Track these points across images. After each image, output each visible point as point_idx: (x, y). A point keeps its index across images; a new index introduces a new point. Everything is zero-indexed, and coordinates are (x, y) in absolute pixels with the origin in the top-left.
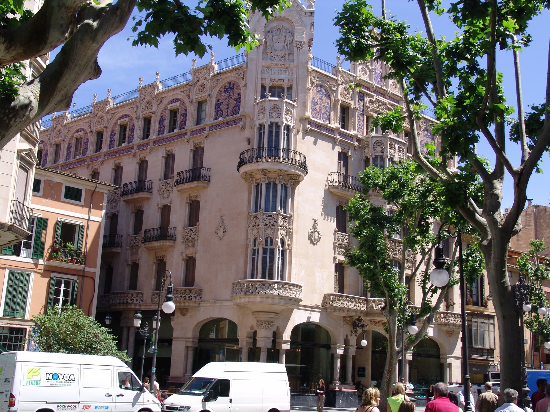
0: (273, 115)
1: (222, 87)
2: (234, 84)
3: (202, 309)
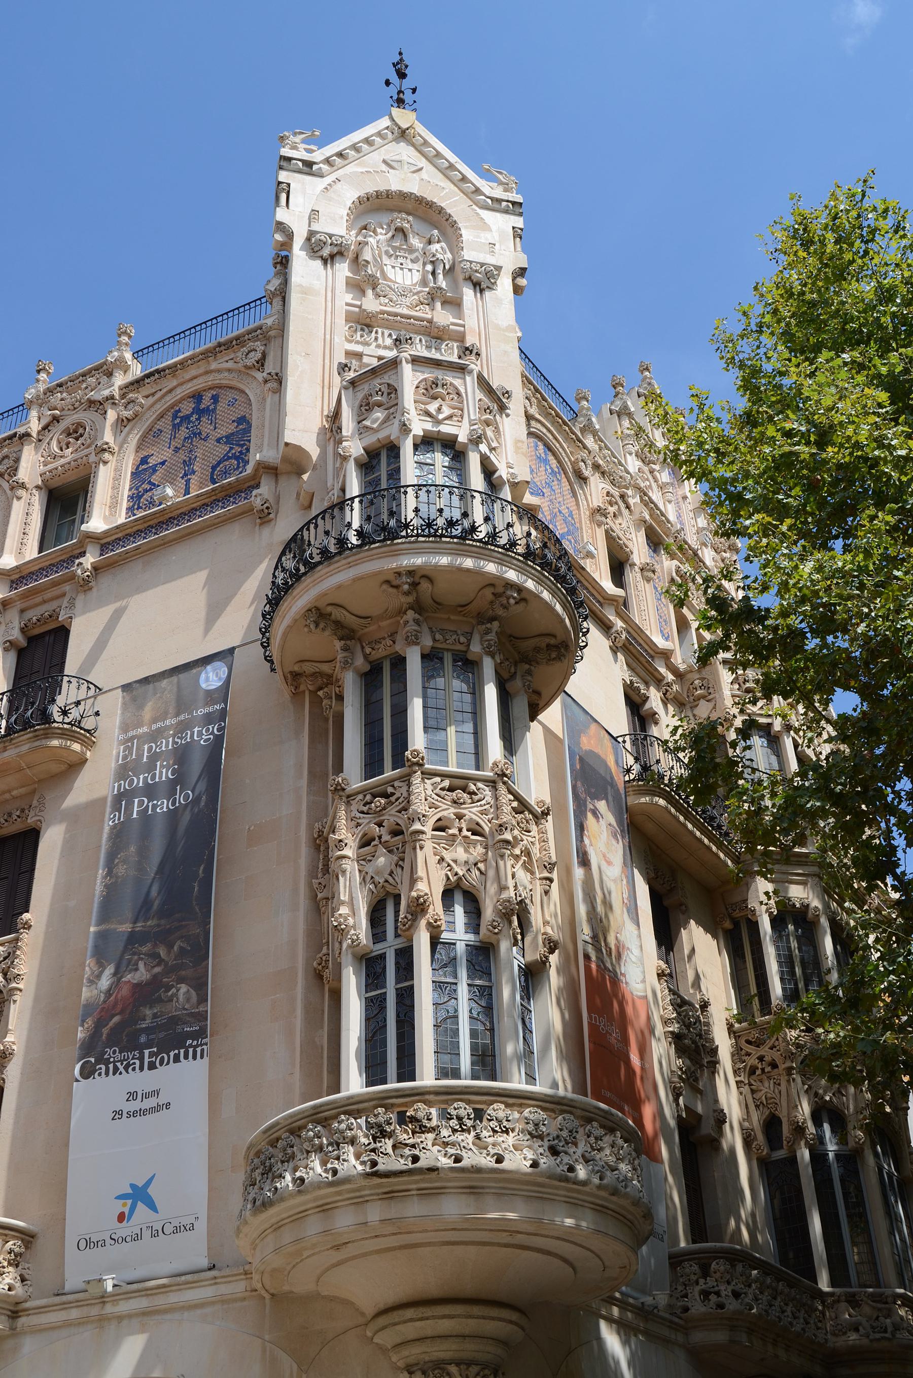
0: (432, 407)
1: (161, 416)
2: (215, 399)
3: (29, 1344)
